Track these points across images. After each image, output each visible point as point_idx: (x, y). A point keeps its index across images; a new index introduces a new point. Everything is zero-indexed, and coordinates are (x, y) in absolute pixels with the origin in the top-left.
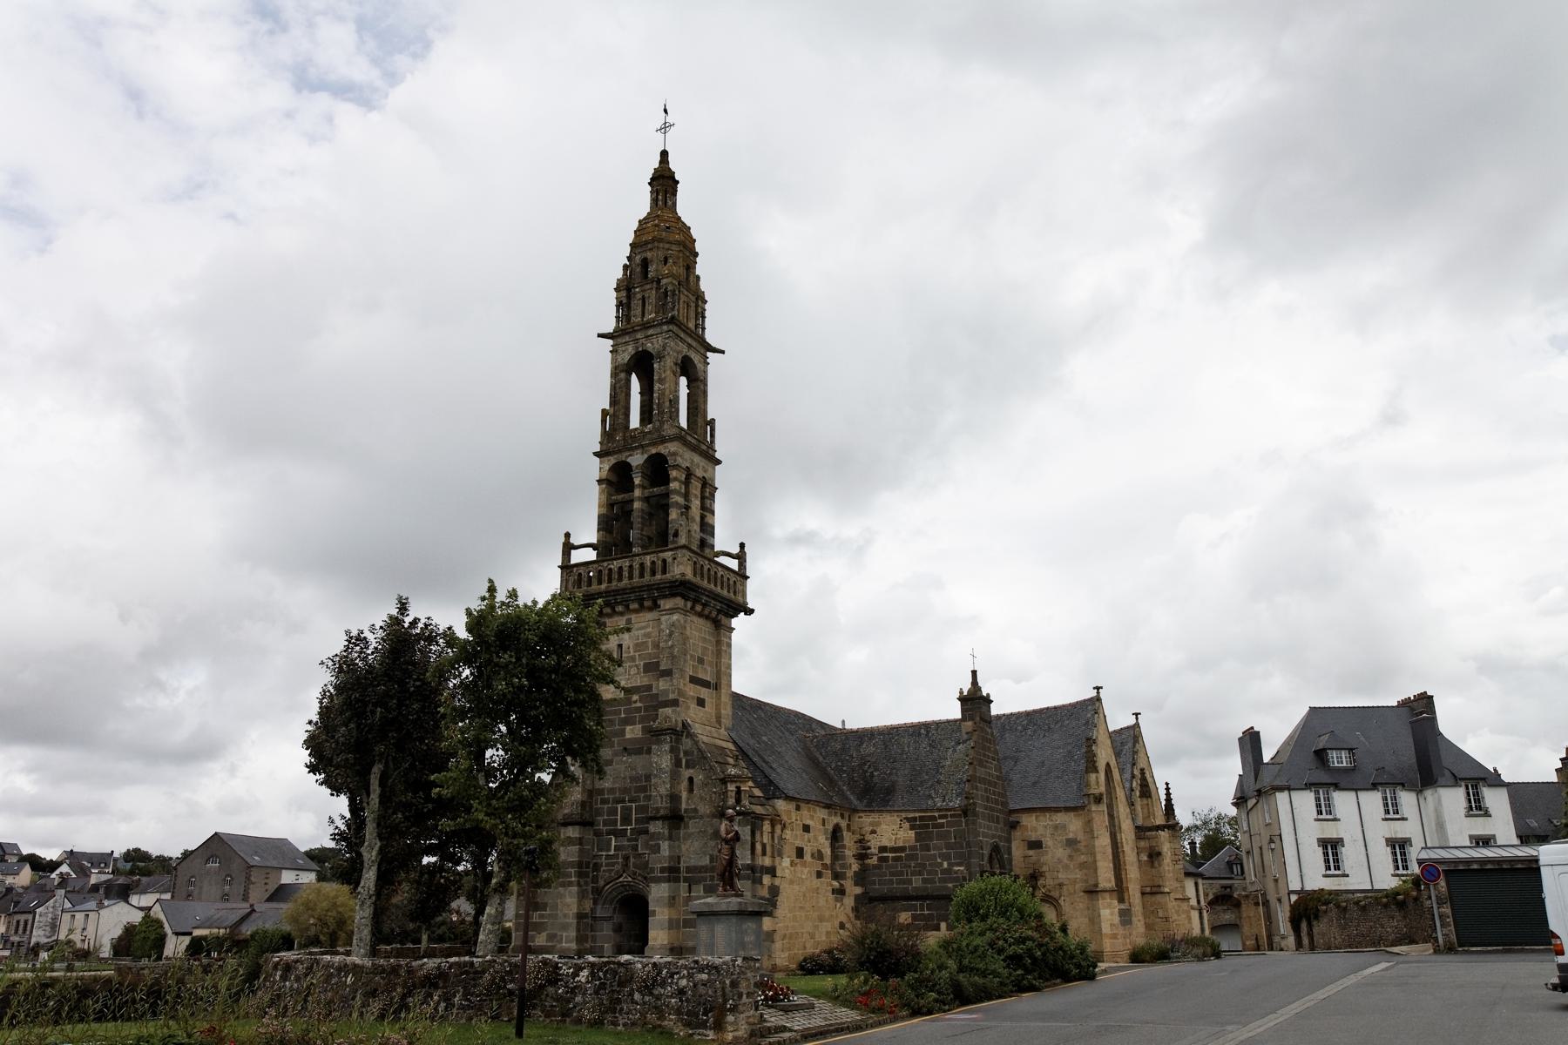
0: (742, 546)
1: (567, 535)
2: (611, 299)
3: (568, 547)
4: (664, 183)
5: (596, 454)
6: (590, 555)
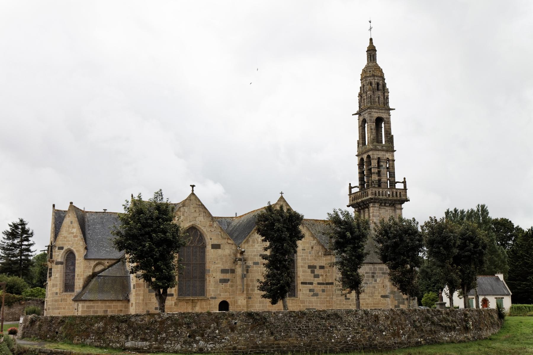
0: (405, 179)
1: (350, 184)
2: (357, 99)
3: (351, 188)
4: (372, 52)
5: (356, 156)
6: (357, 190)
